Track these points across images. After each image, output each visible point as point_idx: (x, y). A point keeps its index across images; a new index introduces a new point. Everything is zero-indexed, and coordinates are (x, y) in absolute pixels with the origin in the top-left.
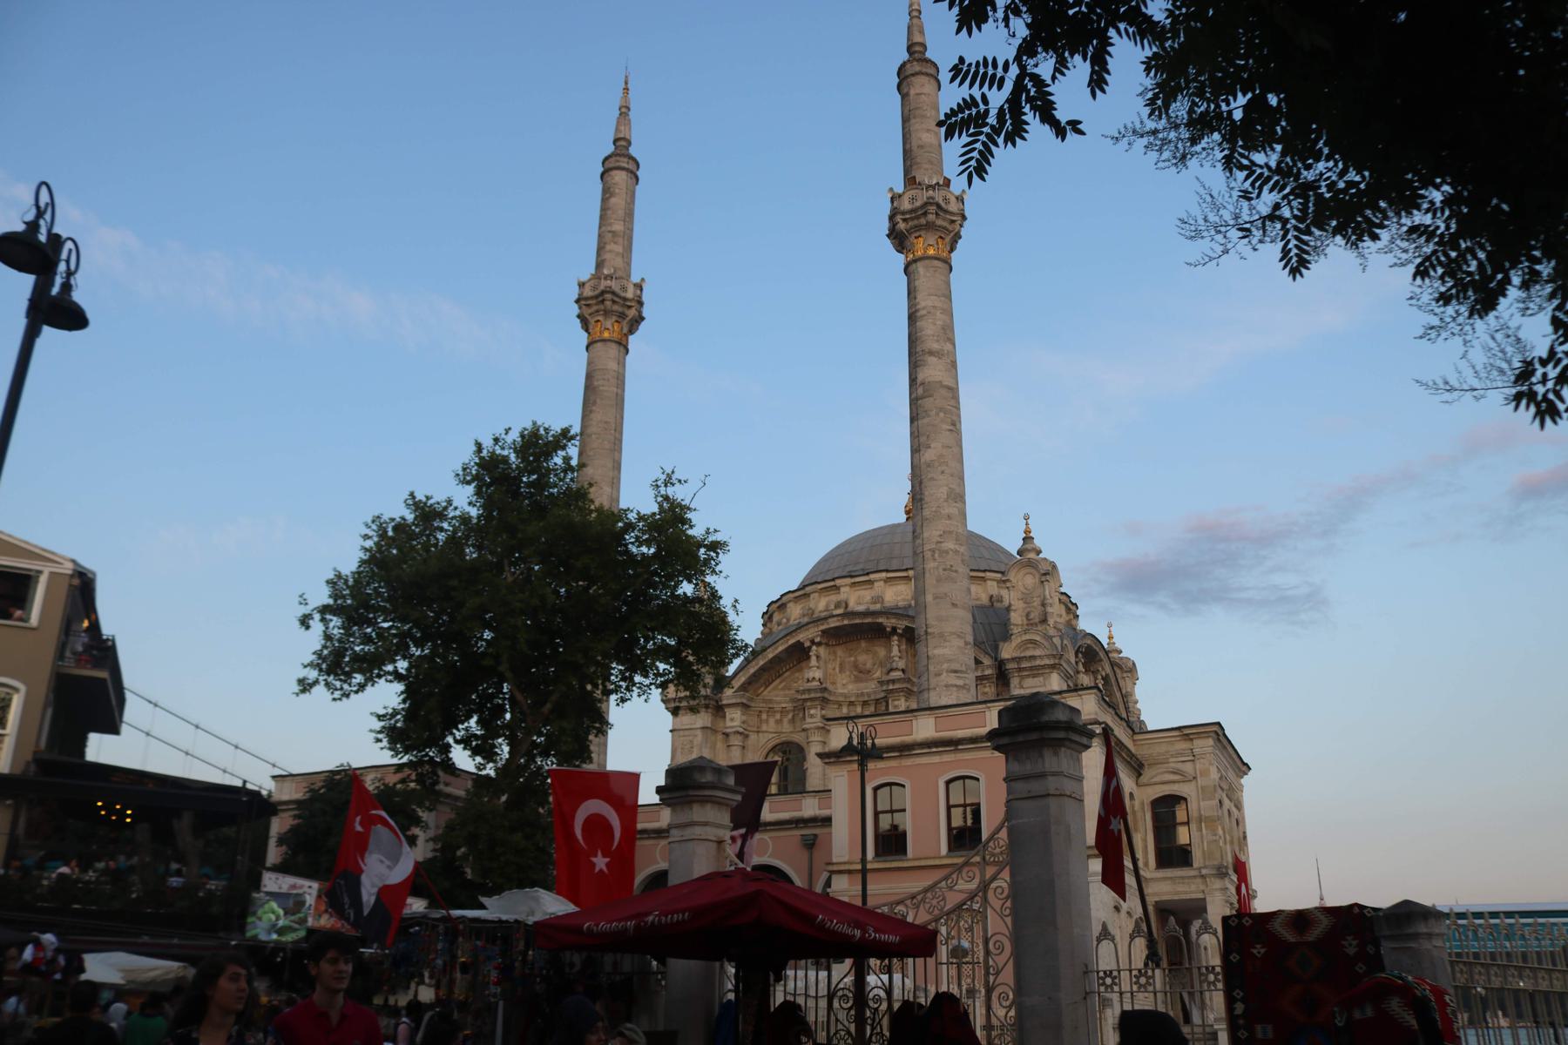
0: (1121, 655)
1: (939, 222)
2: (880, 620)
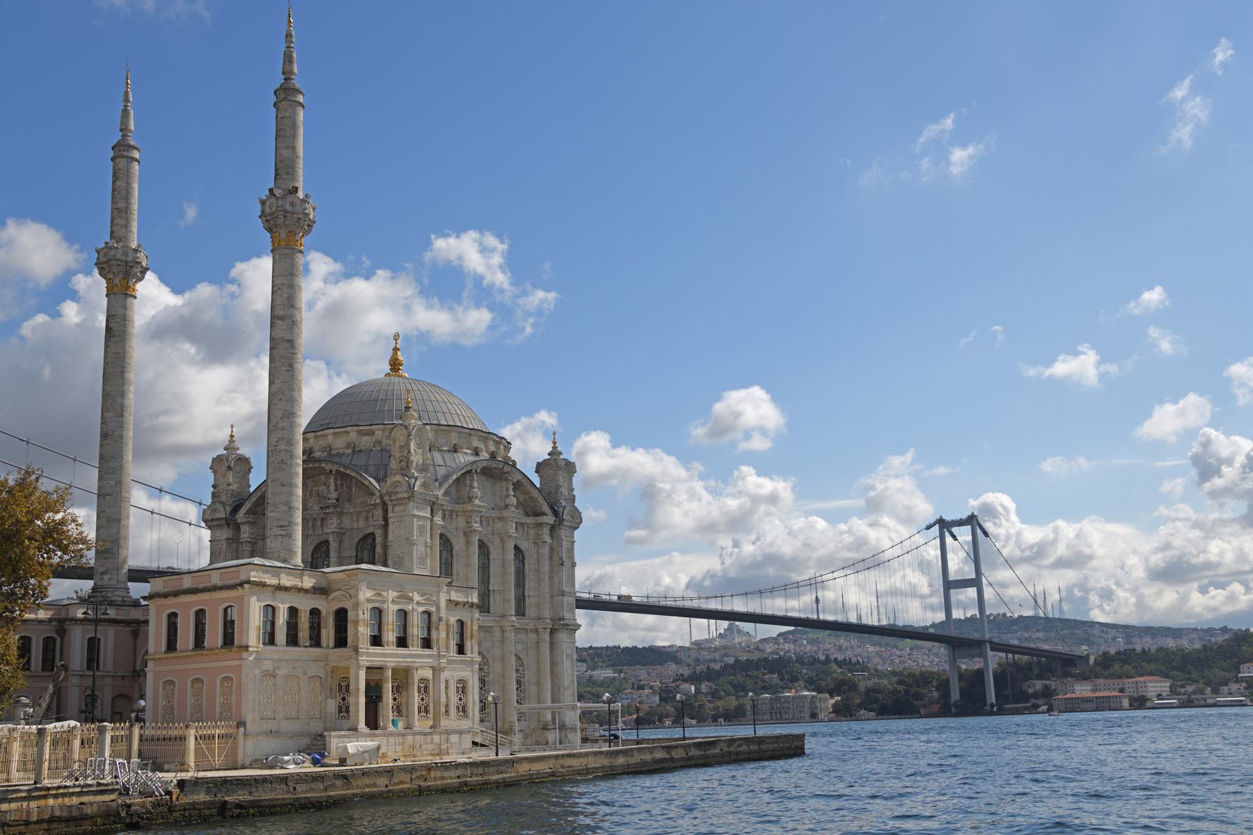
0: (561, 457)
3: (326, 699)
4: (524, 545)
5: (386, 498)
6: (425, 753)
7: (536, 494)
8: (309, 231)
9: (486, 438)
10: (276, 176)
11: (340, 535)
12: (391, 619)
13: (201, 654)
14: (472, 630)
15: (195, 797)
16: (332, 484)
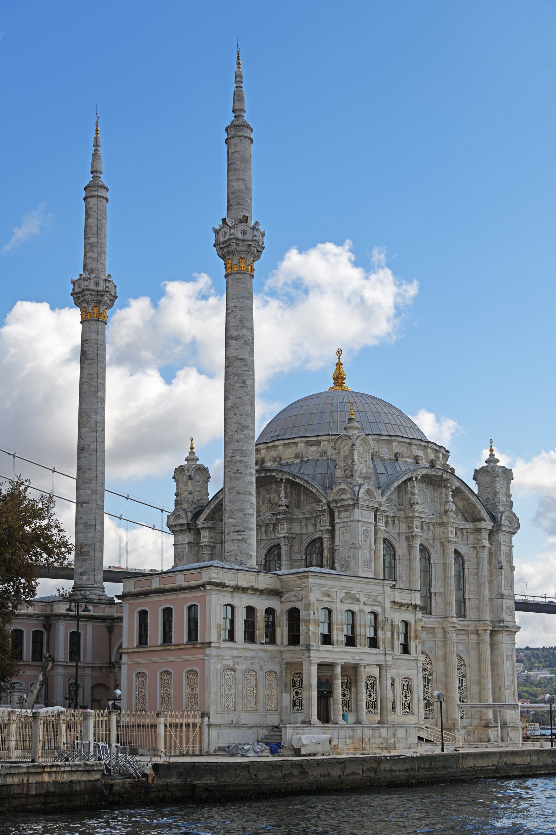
0: (499, 464)
1: (239, 248)
2: (274, 474)
3: (282, 693)
4: (463, 550)
5: (332, 505)
6: (374, 746)
7: (474, 500)
8: (259, 257)
9: (426, 447)
10: (228, 207)
11: (291, 539)
13: (169, 650)
14: (416, 631)
15: (168, 780)
16: (283, 492)
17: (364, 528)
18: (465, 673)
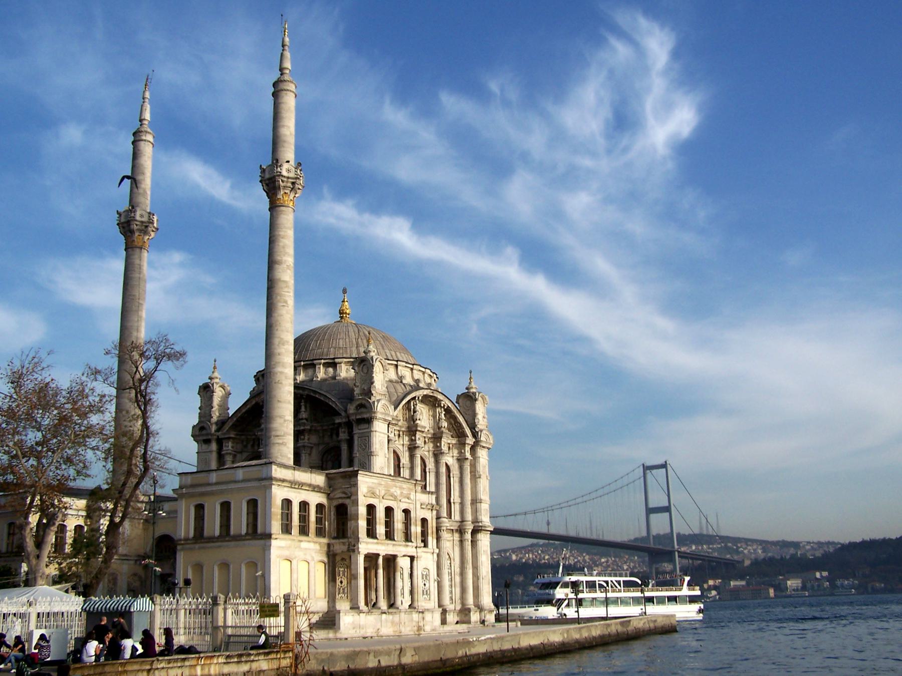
12: (380, 514)
17: (380, 438)
18: (451, 566)
